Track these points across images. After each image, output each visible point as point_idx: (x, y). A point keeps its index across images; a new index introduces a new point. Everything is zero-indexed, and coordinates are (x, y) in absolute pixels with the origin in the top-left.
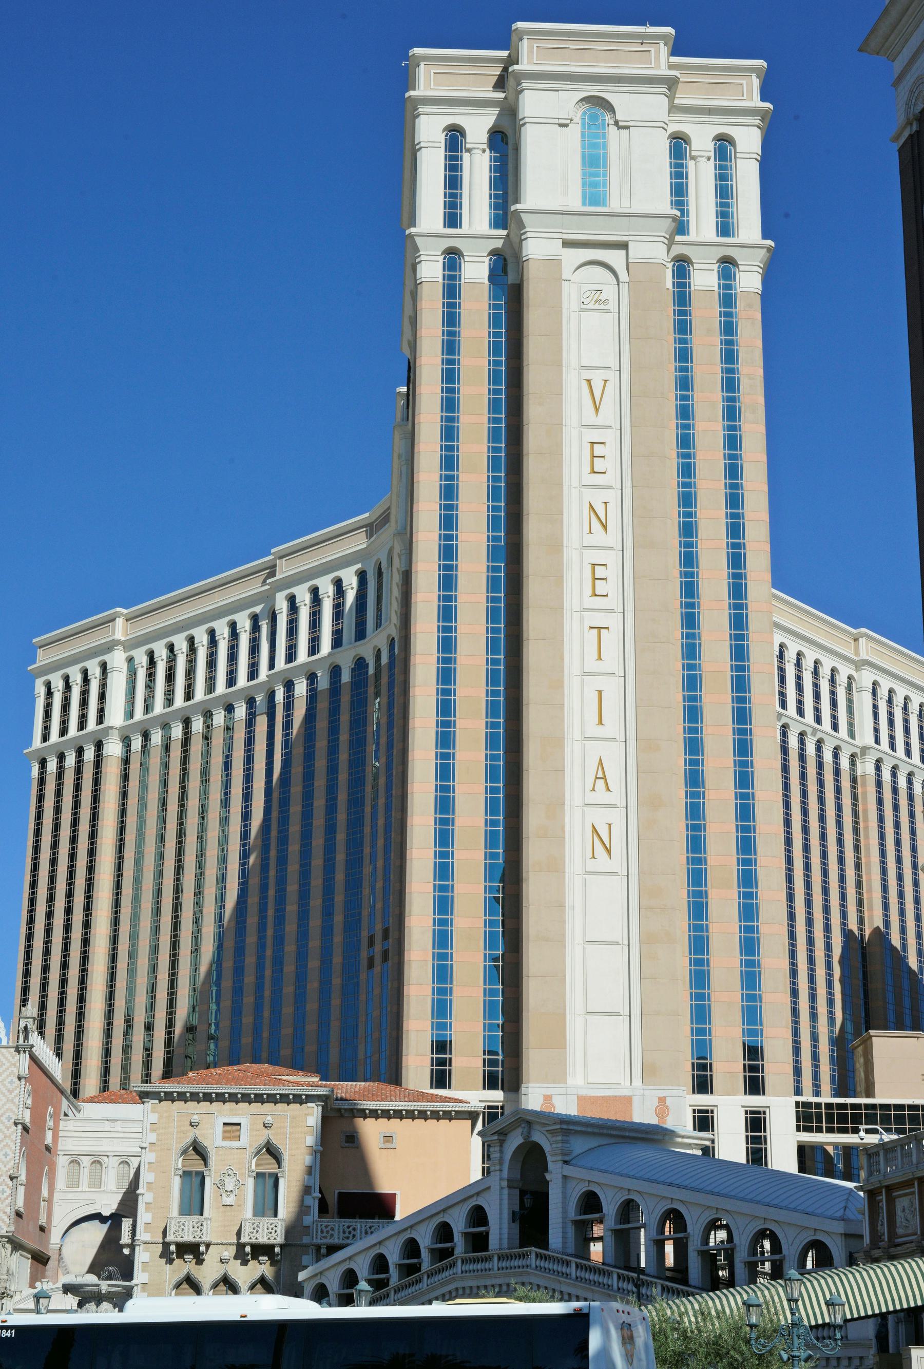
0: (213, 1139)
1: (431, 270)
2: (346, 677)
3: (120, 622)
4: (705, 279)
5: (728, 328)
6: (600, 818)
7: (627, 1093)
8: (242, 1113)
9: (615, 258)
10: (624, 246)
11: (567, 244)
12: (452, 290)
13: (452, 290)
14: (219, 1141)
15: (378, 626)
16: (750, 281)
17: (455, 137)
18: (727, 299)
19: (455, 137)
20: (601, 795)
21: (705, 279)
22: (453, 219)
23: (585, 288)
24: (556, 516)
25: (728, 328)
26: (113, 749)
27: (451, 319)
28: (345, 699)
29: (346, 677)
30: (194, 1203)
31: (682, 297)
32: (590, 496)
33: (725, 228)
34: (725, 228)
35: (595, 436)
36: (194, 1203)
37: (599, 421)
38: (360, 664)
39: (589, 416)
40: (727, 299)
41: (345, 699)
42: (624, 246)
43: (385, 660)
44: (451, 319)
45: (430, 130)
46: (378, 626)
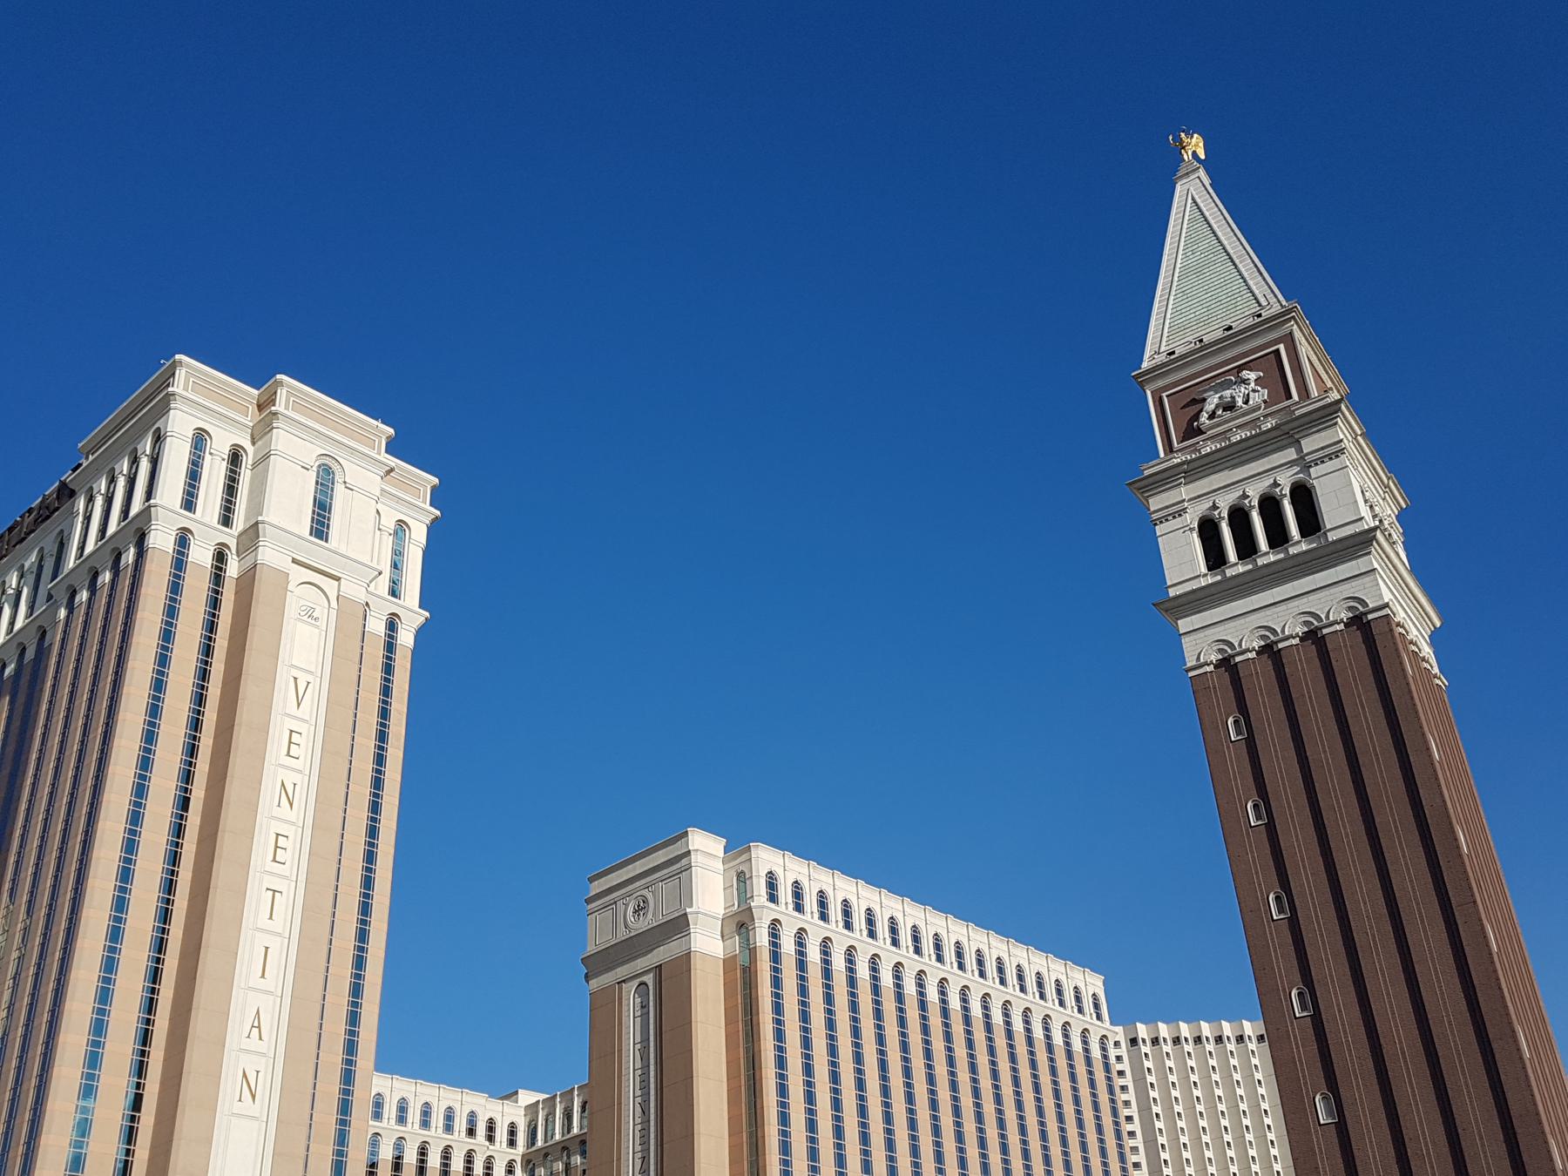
1: (161, 540)
9: (329, 586)
10: (338, 579)
11: (294, 561)
12: (179, 563)
13: (179, 563)
17: (200, 440)
19: (200, 440)
22: (189, 504)
23: (303, 602)
25: (388, 669)
27: (175, 588)
32: (283, 775)
37: (299, 714)
42: (338, 579)
44: (175, 588)
45: (180, 425)
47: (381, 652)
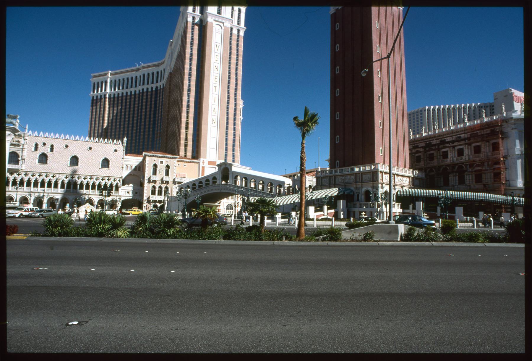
0: (159, 164)
2: (154, 89)
3: (109, 74)
4: (235, 32)
5: (238, 41)
6: (214, 118)
7: (215, 160)
8: (164, 160)
11: (215, 20)
14: (159, 164)
15: (161, 81)
16: (242, 34)
18: (238, 36)
20: (214, 114)
21: (235, 32)
24: (210, 67)
26: (107, 96)
28: (154, 93)
29: (154, 89)
30: (155, 173)
31: (231, 34)
33: (239, 24)
34: (239, 24)
35: (217, 54)
36: (155, 173)
38: (157, 88)
39: (216, 51)
40: (238, 36)
41: (154, 93)
43: (162, 87)
46: (161, 81)
47: (236, 38)
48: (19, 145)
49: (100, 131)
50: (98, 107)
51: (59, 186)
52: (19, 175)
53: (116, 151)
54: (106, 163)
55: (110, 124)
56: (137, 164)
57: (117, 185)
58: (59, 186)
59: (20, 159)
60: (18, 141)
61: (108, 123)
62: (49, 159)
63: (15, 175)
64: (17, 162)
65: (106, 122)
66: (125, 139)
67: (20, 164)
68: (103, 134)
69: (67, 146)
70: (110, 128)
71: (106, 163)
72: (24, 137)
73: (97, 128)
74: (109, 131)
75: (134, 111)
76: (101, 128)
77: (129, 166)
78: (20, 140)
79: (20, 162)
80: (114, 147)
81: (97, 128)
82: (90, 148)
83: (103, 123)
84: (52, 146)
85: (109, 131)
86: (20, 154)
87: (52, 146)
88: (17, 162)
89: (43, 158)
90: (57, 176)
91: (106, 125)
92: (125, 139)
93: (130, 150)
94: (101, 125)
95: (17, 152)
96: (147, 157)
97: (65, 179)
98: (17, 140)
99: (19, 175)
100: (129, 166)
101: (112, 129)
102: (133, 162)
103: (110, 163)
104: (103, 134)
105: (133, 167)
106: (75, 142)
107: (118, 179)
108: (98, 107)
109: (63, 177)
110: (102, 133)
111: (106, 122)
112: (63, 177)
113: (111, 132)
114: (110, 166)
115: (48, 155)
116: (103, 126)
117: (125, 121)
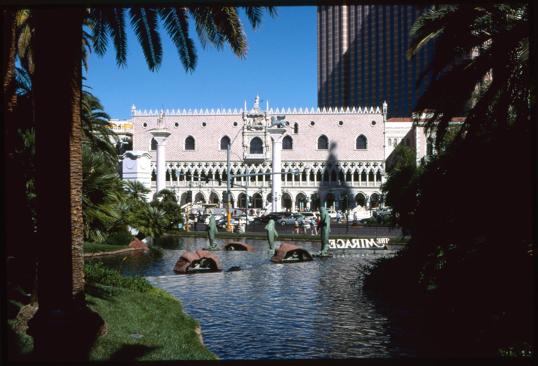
48: (261, 129)
49: (337, 60)
50: (331, 16)
51: (308, 177)
52: (264, 166)
53: (374, 123)
54: (362, 142)
55: (353, 46)
56: (404, 135)
57: (379, 172)
58: (308, 177)
59: (264, 145)
60: (260, 124)
61: (349, 44)
62: (294, 142)
63: (260, 166)
64: (261, 151)
65: (345, 42)
66: (385, 105)
67: (264, 152)
68: (343, 65)
69: (313, 123)
70: (352, 52)
71: (362, 142)
72: (265, 117)
73: (331, 56)
74: (352, 58)
75: (392, 35)
76: (337, 55)
77: (393, 139)
78: (262, 122)
79: (264, 149)
80: (371, 118)
81: (331, 56)
82: (341, 123)
83: (341, 45)
84: (296, 125)
85: (352, 58)
86: (263, 140)
87: (296, 125)
88: (261, 151)
89: (288, 143)
90: (305, 164)
91: (345, 48)
92: (385, 105)
93: (393, 114)
94: (337, 49)
95: (260, 137)
96: (417, 128)
97: (313, 168)
98: (259, 122)
99: (264, 166)
100: (393, 139)
101: (356, 54)
102: (398, 132)
103: (368, 142)
104: (343, 65)
105: (399, 141)
106: (322, 117)
107: (380, 163)
108: (331, 16)
109: (311, 166)
110: (340, 63)
111: (345, 42)
112: (311, 166)
113: (356, 61)
114: (368, 145)
115: (292, 137)
116: (341, 50)
117: (377, 38)
